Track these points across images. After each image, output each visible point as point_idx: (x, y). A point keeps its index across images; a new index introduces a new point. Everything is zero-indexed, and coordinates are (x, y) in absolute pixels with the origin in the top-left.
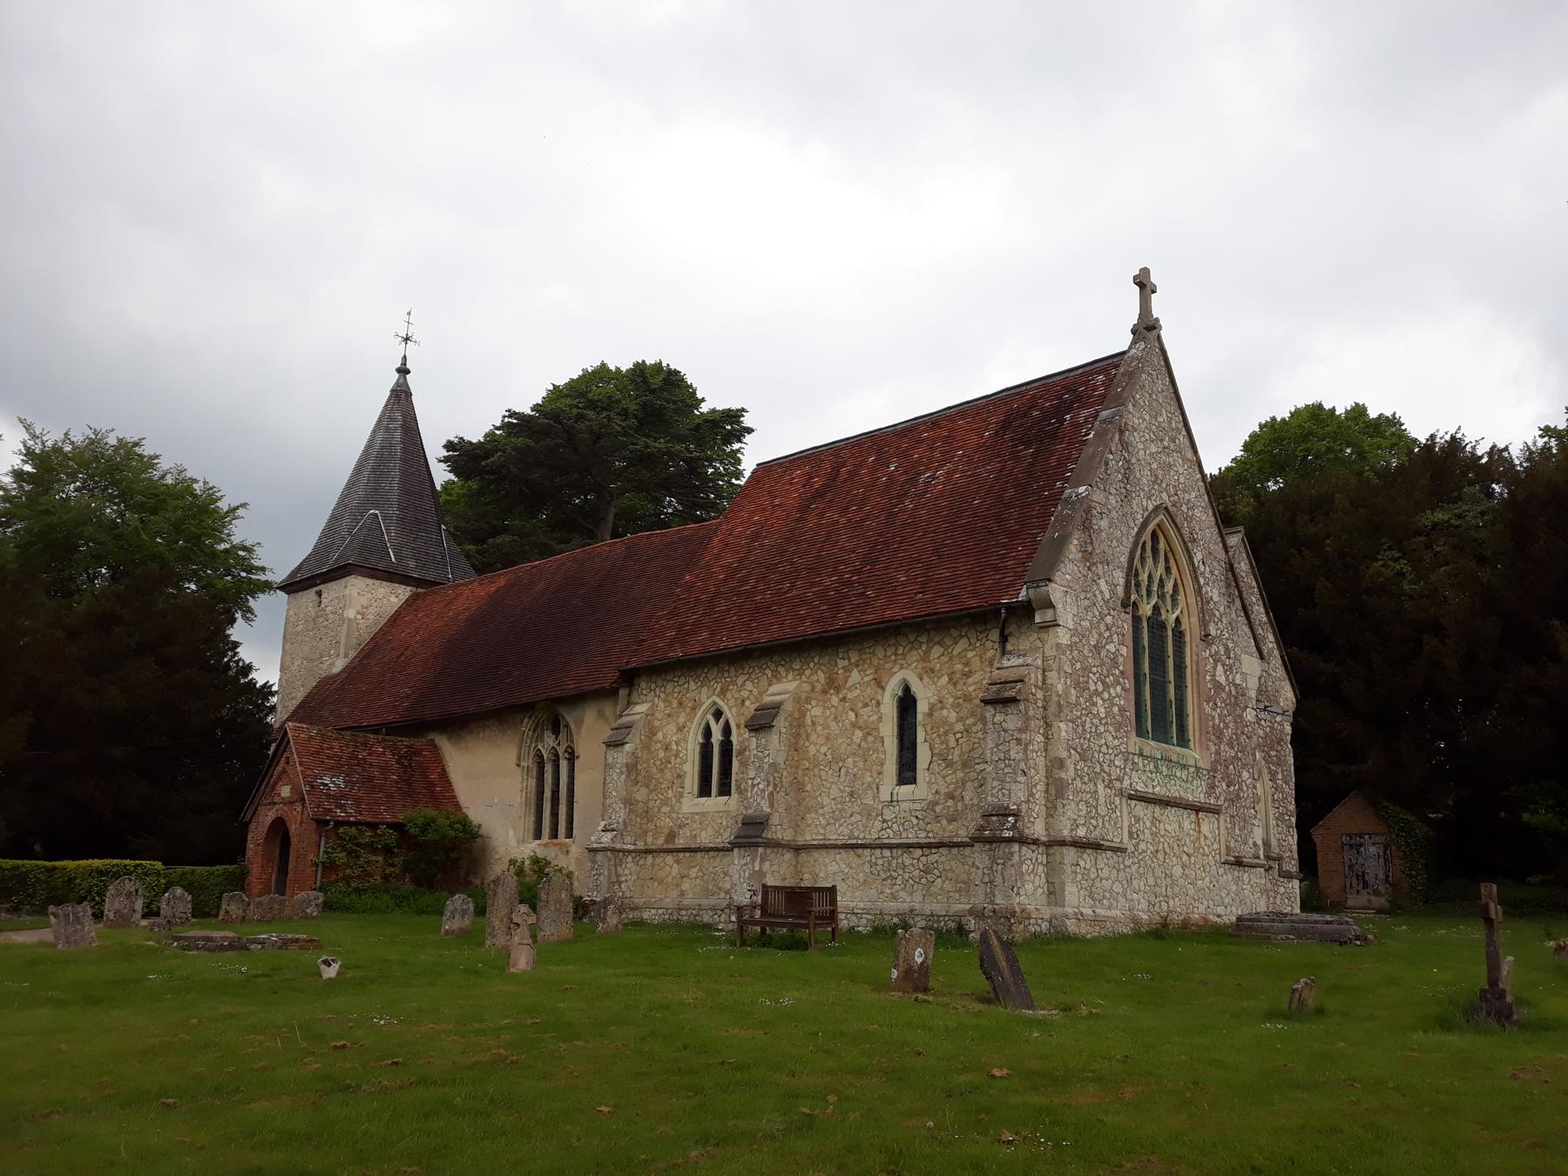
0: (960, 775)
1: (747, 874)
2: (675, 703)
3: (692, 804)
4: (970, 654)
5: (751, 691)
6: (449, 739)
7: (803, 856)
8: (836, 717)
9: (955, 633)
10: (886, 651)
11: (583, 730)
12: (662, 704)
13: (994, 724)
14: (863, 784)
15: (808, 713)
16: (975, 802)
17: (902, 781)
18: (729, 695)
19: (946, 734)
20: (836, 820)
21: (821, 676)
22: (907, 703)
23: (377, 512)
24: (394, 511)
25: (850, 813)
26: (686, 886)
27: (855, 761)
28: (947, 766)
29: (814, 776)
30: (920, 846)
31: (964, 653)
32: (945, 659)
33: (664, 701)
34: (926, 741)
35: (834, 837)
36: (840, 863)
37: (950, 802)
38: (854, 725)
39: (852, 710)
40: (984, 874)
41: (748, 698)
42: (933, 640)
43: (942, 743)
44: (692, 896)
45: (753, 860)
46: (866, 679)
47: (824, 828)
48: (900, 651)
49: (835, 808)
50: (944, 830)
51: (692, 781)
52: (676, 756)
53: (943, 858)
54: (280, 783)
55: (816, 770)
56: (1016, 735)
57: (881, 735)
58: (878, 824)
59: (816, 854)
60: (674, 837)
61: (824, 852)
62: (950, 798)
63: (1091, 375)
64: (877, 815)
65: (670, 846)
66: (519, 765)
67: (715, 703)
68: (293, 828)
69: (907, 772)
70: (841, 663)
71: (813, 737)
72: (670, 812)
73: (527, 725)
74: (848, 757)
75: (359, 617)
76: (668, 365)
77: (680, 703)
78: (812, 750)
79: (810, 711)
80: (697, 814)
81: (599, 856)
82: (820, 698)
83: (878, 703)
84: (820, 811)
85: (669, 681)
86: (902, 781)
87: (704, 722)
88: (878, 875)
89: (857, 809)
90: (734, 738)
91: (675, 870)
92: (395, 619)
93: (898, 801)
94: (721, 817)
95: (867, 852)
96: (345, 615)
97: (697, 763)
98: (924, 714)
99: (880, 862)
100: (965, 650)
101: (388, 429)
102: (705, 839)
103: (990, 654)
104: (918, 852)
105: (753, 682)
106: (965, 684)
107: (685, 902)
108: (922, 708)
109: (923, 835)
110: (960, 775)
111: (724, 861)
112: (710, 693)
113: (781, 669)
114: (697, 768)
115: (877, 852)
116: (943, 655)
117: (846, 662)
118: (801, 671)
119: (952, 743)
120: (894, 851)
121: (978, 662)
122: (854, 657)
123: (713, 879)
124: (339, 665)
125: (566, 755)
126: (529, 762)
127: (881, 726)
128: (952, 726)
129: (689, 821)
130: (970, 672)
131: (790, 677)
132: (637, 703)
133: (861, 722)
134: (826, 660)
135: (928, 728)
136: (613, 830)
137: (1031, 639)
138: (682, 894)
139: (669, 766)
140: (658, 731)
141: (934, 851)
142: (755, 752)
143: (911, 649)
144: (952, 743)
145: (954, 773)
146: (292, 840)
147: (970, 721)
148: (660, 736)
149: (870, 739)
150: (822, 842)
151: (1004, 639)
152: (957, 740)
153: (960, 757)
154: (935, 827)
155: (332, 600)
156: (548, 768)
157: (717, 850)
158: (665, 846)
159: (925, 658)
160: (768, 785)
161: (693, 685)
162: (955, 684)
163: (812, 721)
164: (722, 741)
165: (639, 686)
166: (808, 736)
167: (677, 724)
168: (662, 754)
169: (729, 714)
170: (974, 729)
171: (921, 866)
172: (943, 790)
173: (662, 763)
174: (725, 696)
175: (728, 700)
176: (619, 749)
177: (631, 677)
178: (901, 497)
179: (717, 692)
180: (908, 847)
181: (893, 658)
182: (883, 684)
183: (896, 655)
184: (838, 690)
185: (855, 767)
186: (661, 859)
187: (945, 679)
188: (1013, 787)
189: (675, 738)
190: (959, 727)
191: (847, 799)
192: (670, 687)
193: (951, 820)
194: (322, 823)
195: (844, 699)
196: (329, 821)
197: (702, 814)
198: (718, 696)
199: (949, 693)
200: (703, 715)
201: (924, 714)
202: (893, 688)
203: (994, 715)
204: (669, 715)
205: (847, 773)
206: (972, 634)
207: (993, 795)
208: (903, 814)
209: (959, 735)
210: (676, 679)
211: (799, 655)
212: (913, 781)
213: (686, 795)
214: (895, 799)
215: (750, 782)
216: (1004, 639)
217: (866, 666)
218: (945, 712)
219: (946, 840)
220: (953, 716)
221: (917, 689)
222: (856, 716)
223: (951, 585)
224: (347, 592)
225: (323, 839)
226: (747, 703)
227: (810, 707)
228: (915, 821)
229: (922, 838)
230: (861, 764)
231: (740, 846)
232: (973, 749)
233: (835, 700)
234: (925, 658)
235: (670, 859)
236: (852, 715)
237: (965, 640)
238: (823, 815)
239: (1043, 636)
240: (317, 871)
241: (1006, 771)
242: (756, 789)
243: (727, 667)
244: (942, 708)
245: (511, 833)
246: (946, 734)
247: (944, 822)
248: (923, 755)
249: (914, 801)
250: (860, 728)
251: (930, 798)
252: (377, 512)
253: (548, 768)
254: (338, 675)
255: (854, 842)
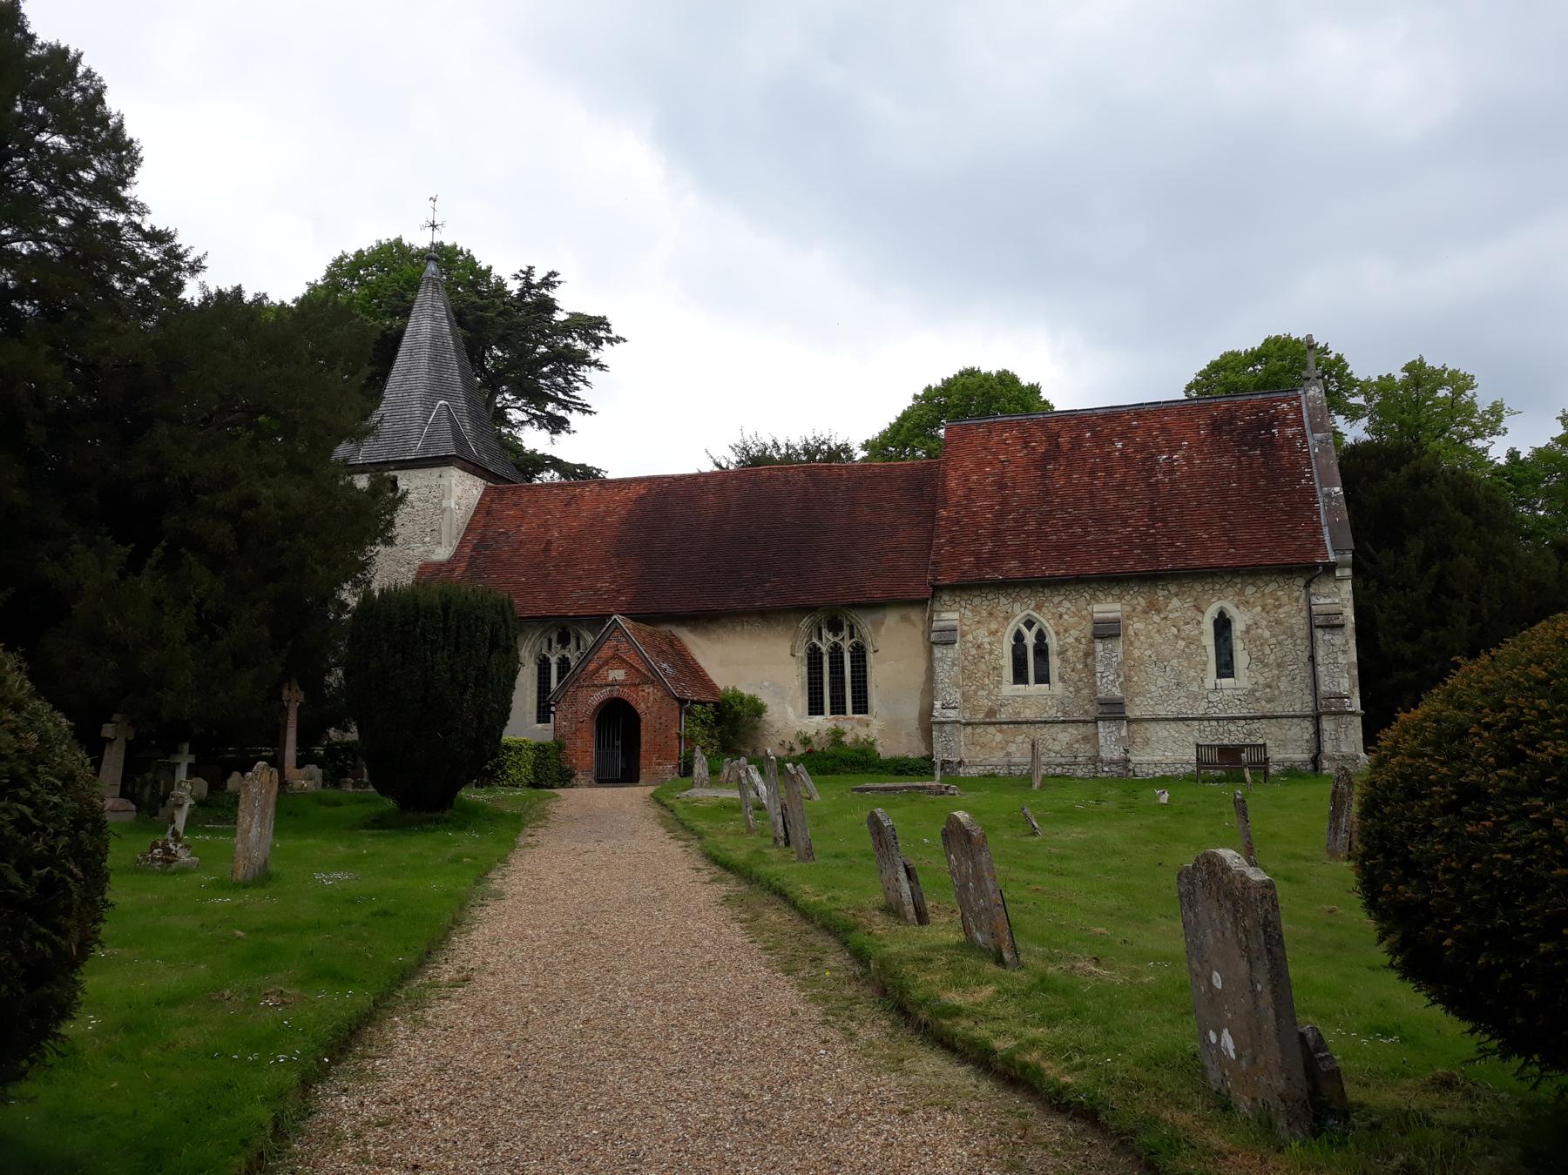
0: (1275, 672)
1: (1113, 739)
2: (985, 614)
3: (1009, 689)
4: (1279, 593)
5: (1069, 608)
6: (691, 631)
7: (1134, 726)
8: (1158, 631)
9: (1266, 578)
10: (1203, 586)
11: (883, 630)
12: (970, 614)
13: (1324, 641)
14: (1188, 677)
15: (1131, 627)
16: (1289, 690)
17: (1220, 675)
18: (1044, 609)
19: (1262, 645)
20: (1164, 702)
21: (1142, 602)
22: (1223, 625)
23: (447, 403)
24: (462, 403)
25: (1177, 696)
26: (1012, 748)
27: (1179, 662)
28: (1264, 666)
29: (1141, 671)
30: (1245, 718)
31: (1274, 592)
32: (1258, 595)
33: (972, 611)
34: (1244, 649)
35: (1162, 713)
36: (1171, 730)
37: (1268, 690)
38: (1176, 637)
39: (1175, 627)
40: (1331, 734)
41: (1066, 613)
42: (1246, 582)
43: (1259, 651)
44: (1019, 756)
45: (1119, 729)
46: (1186, 605)
47: (1152, 707)
48: (1217, 587)
49: (1162, 693)
50: (1264, 708)
51: (1008, 672)
52: (991, 652)
53: (1264, 726)
54: (606, 668)
55: (1142, 667)
56: (1342, 648)
57: (1203, 644)
58: (1204, 704)
59: (1146, 725)
60: (996, 713)
61: (1154, 724)
62: (1267, 687)
63: (1278, 401)
64: (1204, 698)
65: (994, 720)
66: (793, 655)
67: (1028, 615)
68: (641, 708)
69: (1225, 667)
70: (1160, 593)
71: (1137, 644)
72: (988, 695)
73: (805, 622)
74: (1173, 659)
75: (457, 507)
76: (469, 251)
77: (991, 614)
78: (1136, 653)
79: (1132, 625)
80: (1019, 696)
81: (947, 728)
82: (1142, 616)
83: (1199, 623)
84: (1148, 695)
85: (975, 596)
86: (1220, 675)
87: (1016, 629)
88: (1207, 737)
89: (1184, 694)
90: (1053, 643)
91: (999, 737)
92: (484, 510)
93: (1221, 689)
94: (1046, 699)
95: (1196, 723)
96: (444, 505)
97: (1011, 659)
98: (1242, 632)
99: (1209, 729)
100: (1275, 590)
101: (434, 319)
102: (1029, 714)
103: (1297, 594)
104: (1243, 722)
105: (1070, 601)
106: (1276, 613)
107: (1014, 760)
108: (1238, 627)
109: (1245, 711)
110: (1275, 672)
111: (1052, 730)
112: (1024, 607)
113: (1097, 593)
114: (1011, 663)
115: (1206, 723)
116: (1256, 592)
117: (1166, 593)
118: (1121, 596)
119: (1267, 651)
120: (1221, 722)
121: (1287, 599)
122: (1173, 589)
123: (1042, 743)
124: (443, 553)
125: (850, 649)
126: (802, 653)
127: (1202, 638)
128: (1267, 640)
129: (1010, 702)
130: (1280, 605)
131: (1110, 599)
132: (940, 611)
133: (1183, 635)
134: (1146, 589)
135: (1246, 641)
136: (955, 708)
137: (1330, 586)
138: (1009, 754)
139: (983, 660)
140: (967, 634)
141: (1256, 721)
142: (1102, 653)
143: (1227, 587)
144: (1267, 651)
145: (1271, 670)
146: (643, 716)
147: (1284, 637)
148: (969, 637)
149: (1192, 647)
150: (1154, 717)
151: (1307, 585)
152: (1272, 650)
153: (1274, 660)
154: (1257, 706)
155: (417, 488)
156: (826, 659)
157: (1046, 722)
158: (988, 720)
159: (1241, 593)
160: (1119, 676)
161: (1003, 600)
162: (1268, 612)
163: (1135, 633)
164: (1036, 644)
165: (941, 598)
166: (1131, 644)
167: (989, 629)
168: (974, 652)
169: (1046, 621)
170: (1286, 643)
171: (1245, 731)
172: (1261, 681)
173: (975, 658)
174: (1040, 610)
175: (1044, 614)
176: (949, 646)
177: (937, 589)
178: (1151, 472)
179: (1031, 607)
180: (1233, 719)
181: (1211, 591)
182: (1202, 609)
183: (1214, 590)
184: (1159, 611)
185: (1180, 665)
186: (982, 730)
187: (1259, 608)
188: (1341, 681)
189: (987, 640)
190: (1273, 641)
191: (1174, 687)
192: (977, 601)
193: (1269, 701)
194: (682, 702)
195: (1166, 618)
196: (688, 700)
197: (1024, 697)
198: (1032, 610)
199: (1262, 618)
200: (1016, 623)
201: (1242, 632)
202: (1211, 613)
203: (1324, 635)
204: (978, 622)
205: (1173, 670)
206: (1281, 579)
207: (1325, 686)
208: (1227, 698)
209: (1272, 647)
210: (984, 595)
211: (1118, 585)
212: (1231, 675)
213: (1004, 682)
214: (1219, 687)
215: (1099, 675)
216: (1307, 585)
217: (1186, 596)
218: (1260, 631)
219: (1268, 714)
220: (1267, 634)
221: (1232, 612)
222: (1179, 631)
223: (1259, 545)
224: (442, 481)
225: (683, 715)
226: (1065, 617)
227: (1132, 622)
228: (1238, 702)
229: (1244, 712)
230: (1185, 664)
231: (1103, 719)
232: (1285, 656)
233: (1156, 618)
234: (1241, 593)
235: (991, 729)
236: (1175, 630)
237: (1275, 583)
238: (1151, 698)
239: (1338, 584)
240: (680, 743)
241: (1335, 670)
242: (1104, 680)
243: (1041, 590)
244: (1257, 628)
245: (790, 710)
246: (1262, 645)
247: (1263, 703)
248: (1241, 659)
249: (1235, 689)
250: (1183, 639)
251: (1250, 687)
252: (447, 403)
253: (826, 659)
254: (449, 562)
255: (1186, 716)
